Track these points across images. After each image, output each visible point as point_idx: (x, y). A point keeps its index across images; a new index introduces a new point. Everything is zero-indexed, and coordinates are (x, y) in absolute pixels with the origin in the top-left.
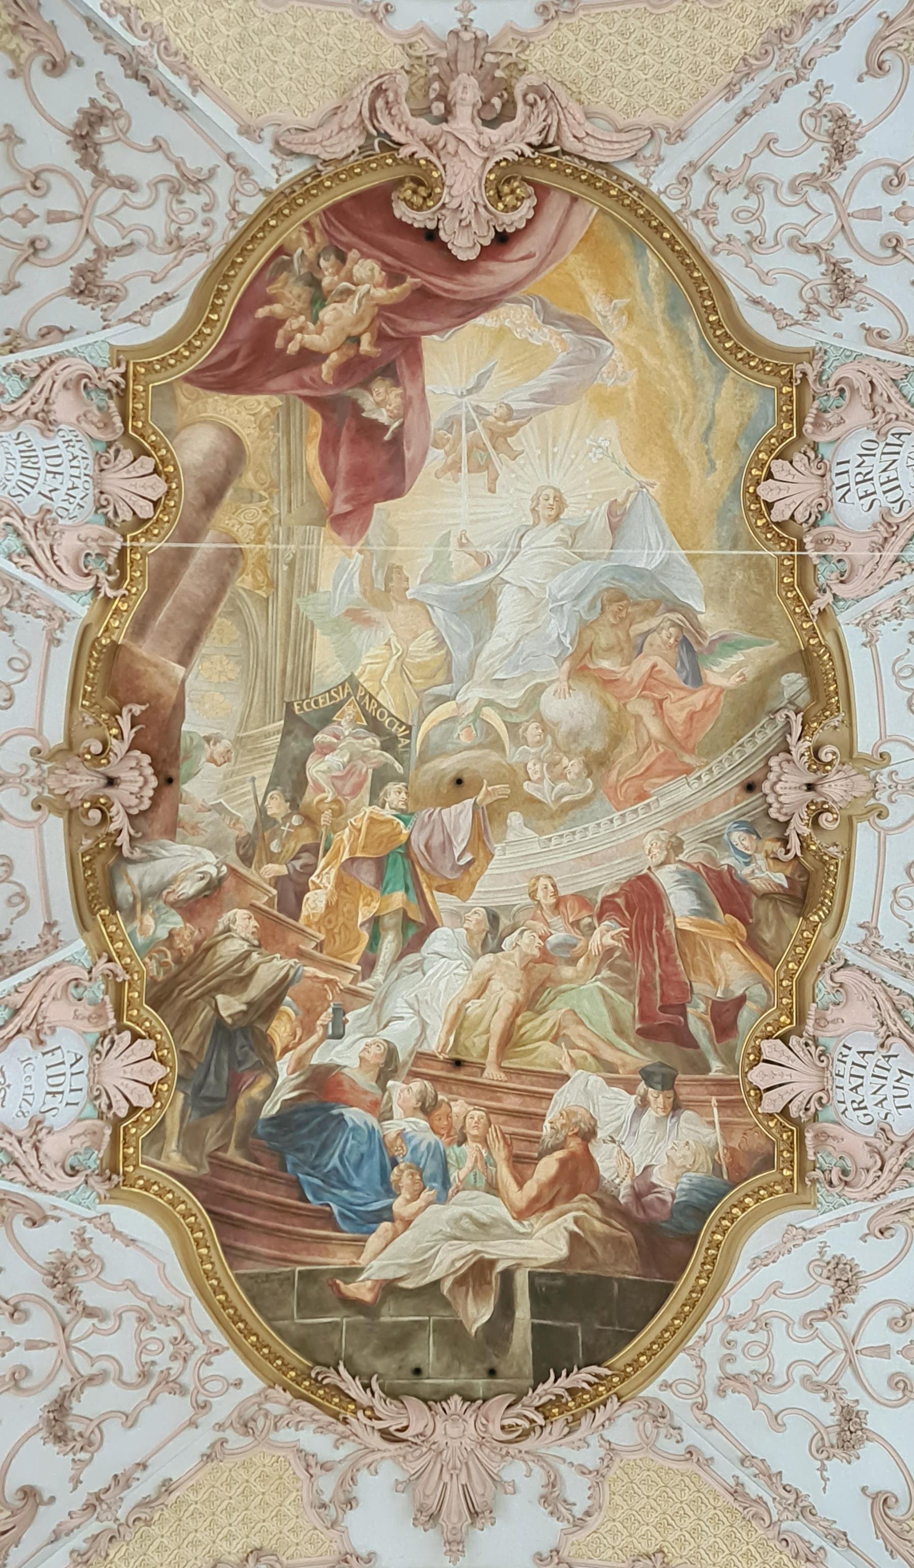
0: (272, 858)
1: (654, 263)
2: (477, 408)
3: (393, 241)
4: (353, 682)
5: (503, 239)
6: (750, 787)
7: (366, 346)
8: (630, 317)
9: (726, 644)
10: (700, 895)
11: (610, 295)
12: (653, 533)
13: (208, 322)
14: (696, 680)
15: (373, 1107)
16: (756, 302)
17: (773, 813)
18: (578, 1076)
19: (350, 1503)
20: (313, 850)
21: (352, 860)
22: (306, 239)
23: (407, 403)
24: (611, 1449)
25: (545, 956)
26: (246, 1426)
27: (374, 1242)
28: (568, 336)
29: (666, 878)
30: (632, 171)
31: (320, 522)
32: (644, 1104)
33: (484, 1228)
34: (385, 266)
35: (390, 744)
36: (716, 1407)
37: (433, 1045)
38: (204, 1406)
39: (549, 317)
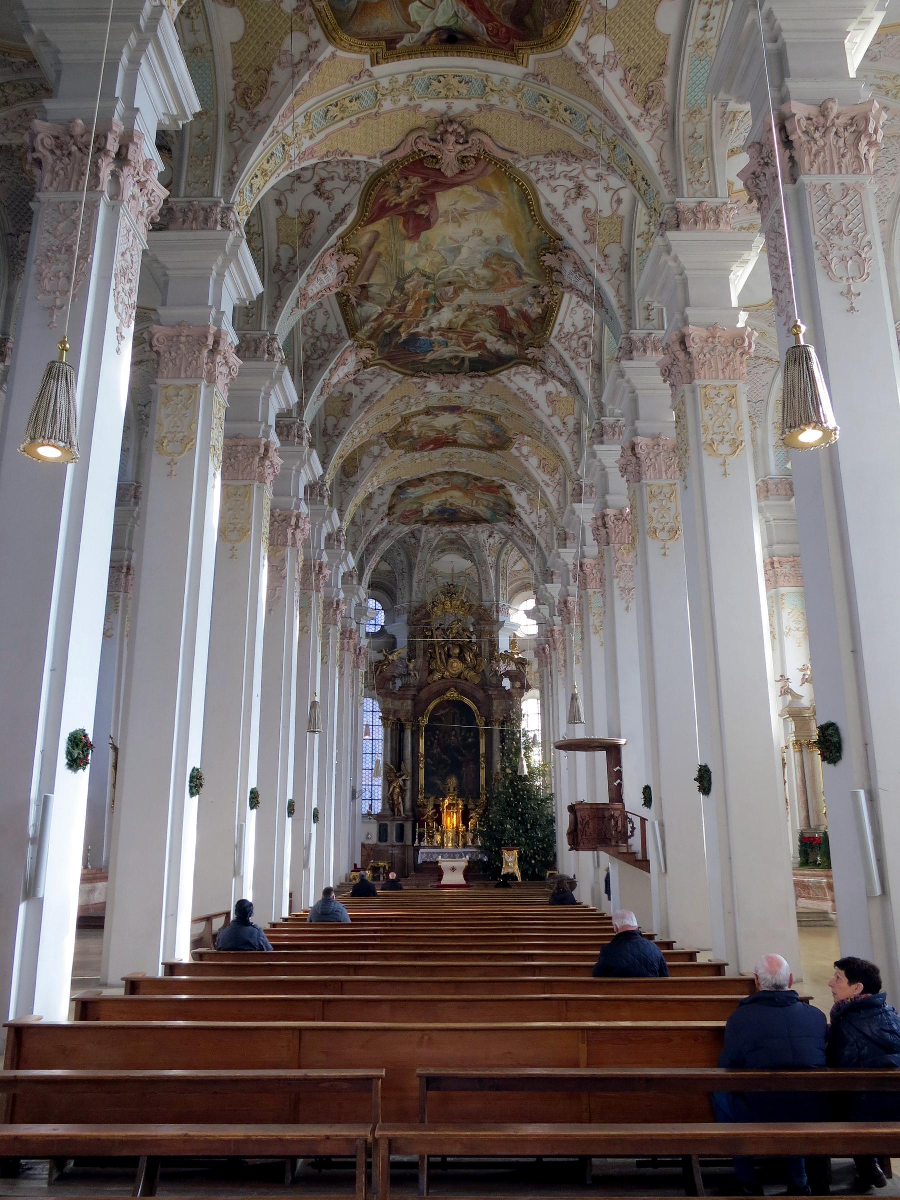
0: (396, 304)
1: (516, 187)
2: (455, 209)
3: (425, 171)
4: (418, 269)
5: (463, 172)
6: (535, 288)
7: (416, 198)
8: (507, 198)
9: (529, 275)
10: (517, 314)
11: (501, 190)
12: (510, 246)
13: (365, 216)
14: (521, 278)
15: (428, 336)
16: (549, 205)
17: (541, 293)
18: (483, 333)
19: (426, 387)
20: (409, 300)
21: (419, 299)
22: (394, 178)
23: (431, 209)
24: (487, 382)
25: (474, 313)
26: (400, 383)
27: (429, 355)
28: (486, 196)
29: (508, 308)
30: (511, 161)
31: (405, 239)
32: (499, 340)
33: (456, 352)
34: (422, 178)
35: (429, 278)
36: (513, 378)
37: (443, 326)
38: (389, 380)
39: (479, 190)
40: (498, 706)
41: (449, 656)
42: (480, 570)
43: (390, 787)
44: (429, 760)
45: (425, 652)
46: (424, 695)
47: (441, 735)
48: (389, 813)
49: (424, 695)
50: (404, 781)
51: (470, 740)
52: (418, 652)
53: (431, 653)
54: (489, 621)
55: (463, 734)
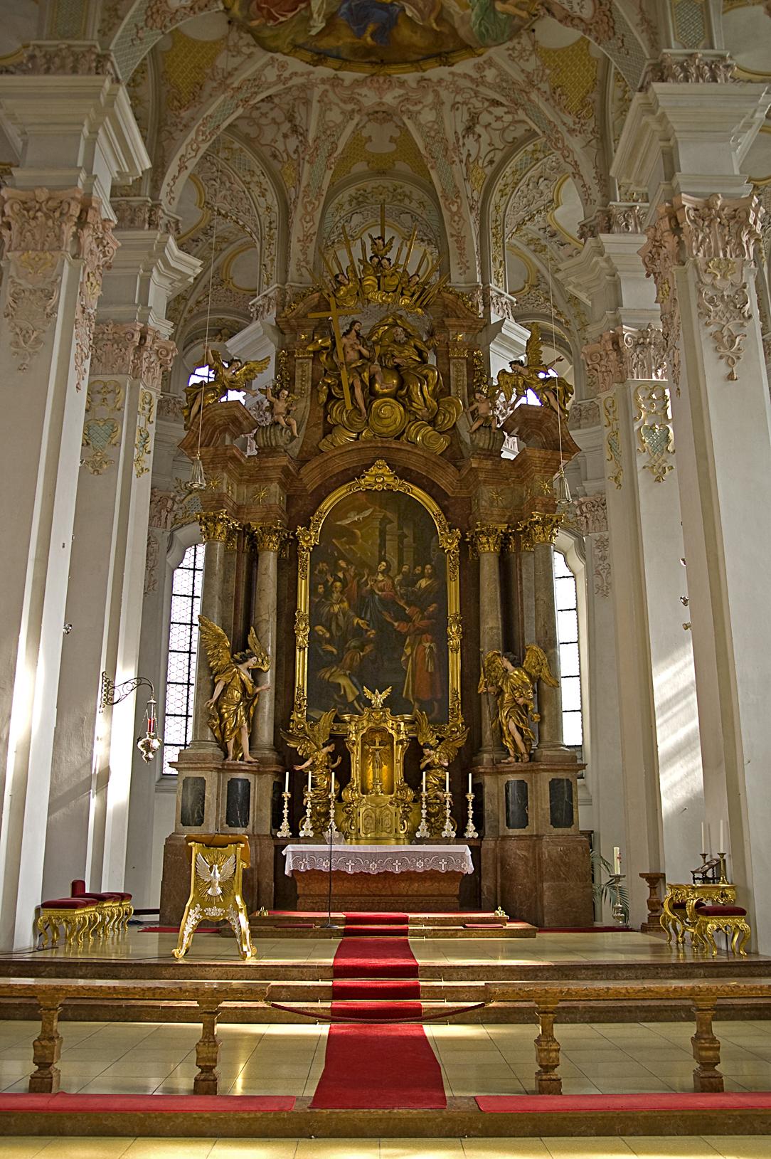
40: (492, 501)
41: (372, 394)
42: (445, 212)
43: (214, 685)
44: (318, 628)
45: (315, 385)
46: (311, 478)
47: (352, 570)
48: (212, 750)
49: (311, 478)
50: (256, 673)
51: (423, 583)
52: (298, 385)
53: (329, 386)
54: (466, 317)
55: (405, 568)
